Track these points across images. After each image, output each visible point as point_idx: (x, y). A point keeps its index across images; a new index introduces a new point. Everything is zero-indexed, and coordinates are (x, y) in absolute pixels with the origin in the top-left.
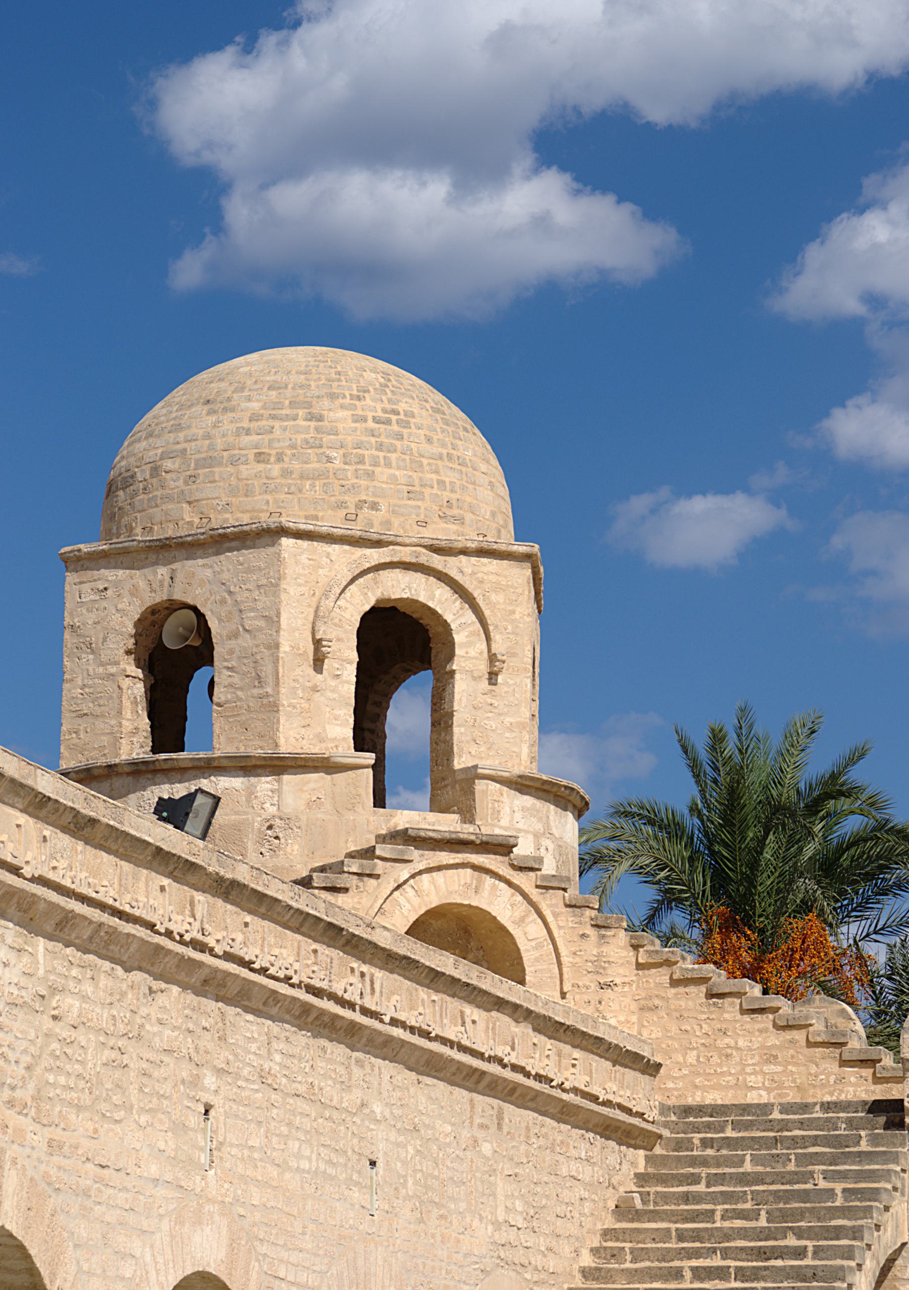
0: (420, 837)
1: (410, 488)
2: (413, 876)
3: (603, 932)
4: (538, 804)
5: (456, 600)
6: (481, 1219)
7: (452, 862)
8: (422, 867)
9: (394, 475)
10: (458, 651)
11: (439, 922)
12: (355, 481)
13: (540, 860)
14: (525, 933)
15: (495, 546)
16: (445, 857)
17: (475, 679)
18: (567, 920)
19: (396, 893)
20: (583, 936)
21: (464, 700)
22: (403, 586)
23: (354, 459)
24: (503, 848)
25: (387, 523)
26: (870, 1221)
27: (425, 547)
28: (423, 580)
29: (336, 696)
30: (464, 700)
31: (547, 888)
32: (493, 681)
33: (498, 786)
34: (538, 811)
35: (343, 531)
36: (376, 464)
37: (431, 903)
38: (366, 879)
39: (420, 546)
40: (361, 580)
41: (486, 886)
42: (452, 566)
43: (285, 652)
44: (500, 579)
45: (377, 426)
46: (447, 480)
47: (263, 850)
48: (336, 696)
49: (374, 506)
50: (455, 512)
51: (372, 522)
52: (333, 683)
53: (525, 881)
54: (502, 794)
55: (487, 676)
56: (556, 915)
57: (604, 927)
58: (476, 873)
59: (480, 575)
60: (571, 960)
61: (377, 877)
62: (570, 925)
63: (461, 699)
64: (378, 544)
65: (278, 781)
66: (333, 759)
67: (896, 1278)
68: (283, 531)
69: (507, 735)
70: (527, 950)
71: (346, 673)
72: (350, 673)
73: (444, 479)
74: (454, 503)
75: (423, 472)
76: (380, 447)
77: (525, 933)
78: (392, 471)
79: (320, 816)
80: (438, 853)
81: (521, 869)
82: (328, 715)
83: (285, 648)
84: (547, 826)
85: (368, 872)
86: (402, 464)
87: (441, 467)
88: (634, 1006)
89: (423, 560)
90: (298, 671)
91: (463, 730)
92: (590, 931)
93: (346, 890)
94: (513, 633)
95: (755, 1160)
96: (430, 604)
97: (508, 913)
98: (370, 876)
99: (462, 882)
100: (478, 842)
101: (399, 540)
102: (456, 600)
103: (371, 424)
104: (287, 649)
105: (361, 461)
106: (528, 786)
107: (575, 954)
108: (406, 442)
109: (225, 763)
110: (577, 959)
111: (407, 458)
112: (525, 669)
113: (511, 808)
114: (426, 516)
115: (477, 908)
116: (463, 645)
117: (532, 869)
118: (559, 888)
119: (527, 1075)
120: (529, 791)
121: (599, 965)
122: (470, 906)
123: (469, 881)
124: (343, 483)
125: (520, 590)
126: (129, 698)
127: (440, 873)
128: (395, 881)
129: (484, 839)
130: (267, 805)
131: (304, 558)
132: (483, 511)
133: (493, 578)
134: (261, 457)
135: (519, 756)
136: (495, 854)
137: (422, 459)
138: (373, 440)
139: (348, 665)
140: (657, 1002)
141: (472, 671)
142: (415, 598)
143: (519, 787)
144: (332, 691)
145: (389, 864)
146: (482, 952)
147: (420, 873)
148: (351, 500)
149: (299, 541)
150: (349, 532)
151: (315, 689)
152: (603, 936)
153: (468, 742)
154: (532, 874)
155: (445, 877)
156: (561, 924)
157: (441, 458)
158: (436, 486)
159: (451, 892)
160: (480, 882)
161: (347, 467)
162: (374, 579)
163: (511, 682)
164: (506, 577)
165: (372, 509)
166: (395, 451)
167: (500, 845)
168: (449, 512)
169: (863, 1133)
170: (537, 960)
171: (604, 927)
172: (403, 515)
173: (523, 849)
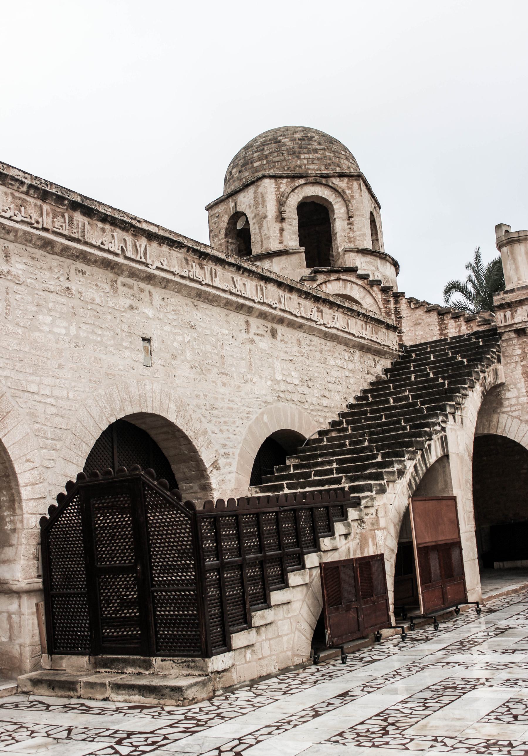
6: (261, 377)
13: (368, 275)
52: (289, 227)
84: (377, 268)
88: (412, 324)
92: (391, 299)
95: (434, 357)
96: (323, 196)
116: (337, 209)
117: (365, 279)
119: (296, 317)
121: (397, 312)
134: (260, 159)
140: (420, 321)
154: (366, 281)
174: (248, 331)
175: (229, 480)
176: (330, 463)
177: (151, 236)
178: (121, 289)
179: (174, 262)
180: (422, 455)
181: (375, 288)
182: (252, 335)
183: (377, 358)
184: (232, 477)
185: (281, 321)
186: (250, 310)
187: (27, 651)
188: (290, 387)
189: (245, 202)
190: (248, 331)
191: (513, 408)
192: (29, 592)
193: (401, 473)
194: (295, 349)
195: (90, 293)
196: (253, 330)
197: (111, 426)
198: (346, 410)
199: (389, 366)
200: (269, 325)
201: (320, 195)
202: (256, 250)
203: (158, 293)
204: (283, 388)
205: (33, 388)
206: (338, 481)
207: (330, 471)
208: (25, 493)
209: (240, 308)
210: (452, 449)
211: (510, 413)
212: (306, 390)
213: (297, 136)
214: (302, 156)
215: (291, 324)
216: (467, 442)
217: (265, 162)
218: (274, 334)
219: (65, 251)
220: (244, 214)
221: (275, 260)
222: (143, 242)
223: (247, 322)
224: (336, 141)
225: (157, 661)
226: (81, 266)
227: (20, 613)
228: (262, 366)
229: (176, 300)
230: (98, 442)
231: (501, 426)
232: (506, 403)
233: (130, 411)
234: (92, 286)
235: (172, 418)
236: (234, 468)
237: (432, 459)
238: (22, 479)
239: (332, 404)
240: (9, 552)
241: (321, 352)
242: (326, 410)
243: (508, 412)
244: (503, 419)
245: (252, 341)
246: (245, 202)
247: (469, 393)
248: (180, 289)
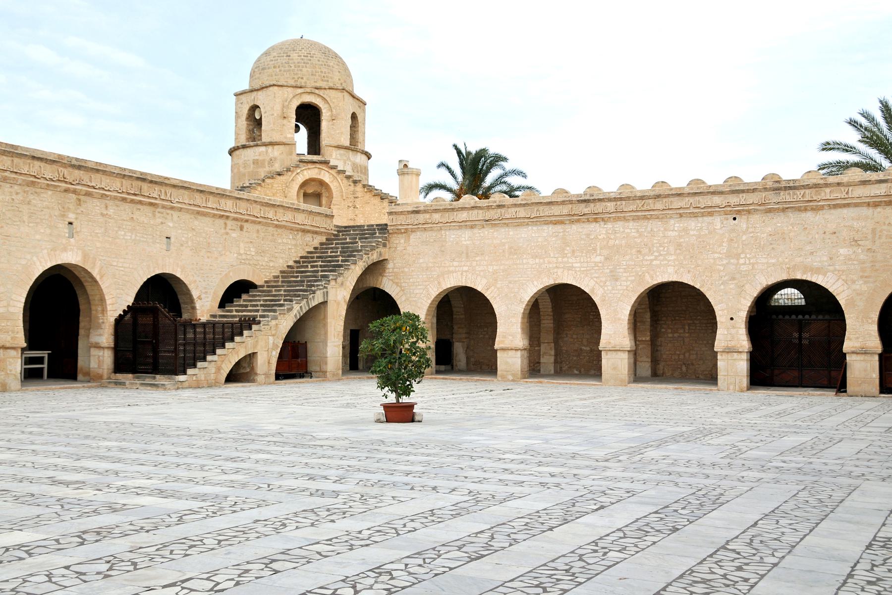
25: (306, 83)
53: (333, 172)
92: (352, 184)
121: (354, 192)
148: (296, 77)
173: (331, 164)
174: (225, 228)
175: (205, 305)
176: (259, 301)
177: (174, 186)
178: (158, 215)
179: (186, 197)
180: (307, 302)
181: (341, 176)
182: (227, 230)
183: (315, 236)
184: (208, 304)
185: (247, 221)
186: (228, 217)
187: (105, 372)
188: (248, 257)
189: (260, 99)
190: (225, 228)
192: (108, 348)
193: (290, 310)
194: (255, 235)
195: (142, 219)
196: (229, 227)
197: (148, 279)
198: (286, 269)
199: (324, 241)
200: (239, 224)
202: (265, 138)
203: (176, 214)
204: (244, 257)
205: (115, 264)
206: (258, 311)
207: (257, 305)
208: (109, 308)
209: (221, 216)
210: (331, 298)
212: (259, 258)
213: (304, 52)
215: (254, 222)
217: (278, 70)
218: (242, 228)
219: (132, 201)
220: (258, 107)
221: (276, 147)
222: (169, 190)
223: (225, 224)
224: (336, 56)
225: (158, 376)
226: (139, 206)
227: (103, 356)
229: (186, 217)
230: (142, 287)
232: (387, 271)
233: (157, 272)
234: (143, 215)
235: (178, 275)
236: (210, 299)
237: (313, 304)
238: (108, 302)
239: (277, 265)
240: (101, 331)
241: (273, 235)
244: (385, 280)
245: (227, 234)
246: (260, 99)
247: (352, 267)
248: (188, 211)
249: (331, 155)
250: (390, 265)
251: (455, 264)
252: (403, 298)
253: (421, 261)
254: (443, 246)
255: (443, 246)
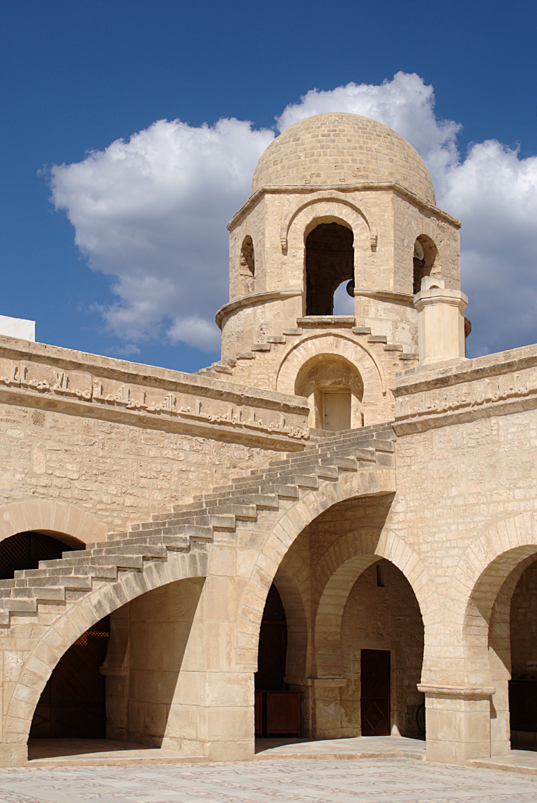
0: (303, 322)
1: (337, 164)
2: (303, 341)
3: (406, 362)
4: (396, 307)
5: (354, 213)
7: (321, 333)
8: (306, 337)
9: (328, 160)
10: (355, 238)
11: (333, 365)
12: (309, 165)
14: (363, 366)
15: (371, 185)
16: (319, 331)
17: (364, 250)
18: (386, 358)
19: (295, 351)
20: (395, 365)
21: (359, 261)
22: (326, 210)
23: (309, 155)
24: (350, 325)
26: (314, 474)
27: (335, 189)
28: (337, 206)
29: (294, 265)
30: (359, 261)
31: (374, 342)
32: (374, 250)
33: (367, 298)
34: (396, 310)
35: (293, 187)
36: (319, 155)
37: (312, 354)
38: (278, 345)
39: (333, 189)
40: (305, 210)
41: (341, 344)
42: (348, 197)
43: (268, 248)
44: (376, 200)
45: (323, 138)
46: (358, 159)
47: (259, 340)
48: (294, 265)
49: (318, 175)
50: (362, 173)
51: (315, 182)
53: (363, 340)
54: (370, 303)
55: (370, 248)
56: (379, 356)
57: (406, 360)
58: (336, 338)
59: (366, 200)
60: (388, 377)
61: (285, 343)
62: (388, 360)
63: (357, 261)
64: (312, 191)
65: (264, 307)
66: (281, 293)
67: (392, 512)
68: (264, 192)
69: (382, 275)
70: (364, 374)
71: (298, 254)
72: (301, 255)
73: (356, 158)
74: (362, 169)
75: (344, 156)
76: (322, 147)
77: (363, 366)
78: (327, 158)
79: (279, 321)
80: (315, 330)
81: (359, 334)
82: (290, 275)
83: (268, 245)
85: (278, 341)
86: (332, 153)
87: (355, 153)
89: (334, 196)
90: (275, 256)
91: (359, 275)
93: (269, 351)
94: (383, 226)
96: (341, 217)
97: (354, 356)
98: (280, 343)
99: (329, 343)
100: (333, 322)
101: (321, 188)
102: (354, 213)
103: (320, 138)
104: (269, 246)
105: (313, 155)
106: (388, 298)
107: (390, 374)
108: (336, 143)
109: (245, 303)
110: (392, 376)
111: (336, 150)
112: (391, 243)
113: (376, 309)
114: (344, 177)
115: (337, 355)
116: (356, 234)
118: (380, 342)
120: (389, 300)
122: (333, 354)
123: (332, 342)
124: (304, 167)
125: (387, 205)
126: (243, 285)
127: (317, 339)
128: (292, 345)
129: (336, 320)
130: (260, 319)
131: (276, 203)
132: (382, 172)
133: (372, 200)
135: (388, 285)
136: (345, 328)
137: (344, 150)
138: (319, 144)
139: (300, 251)
141: (363, 246)
142: (333, 215)
143: (381, 298)
144: (292, 263)
145: (290, 337)
146: (357, 378)
147: (306, 340)
148: (308, 174)
149: (274, 195)
150: (296, 187)
151: (284, 263)
152: (406, 364)
153: (362, 281)
155: (319, 341)
156: (382, 359)
157: (355, 148)
158: (350, 161)
159: (323, 348)
160: (338, 342)
161: (306, 159)
162: (312, 208)
163: (383, 249)
164: (379, 199)
165: (317, 176)
166: (329, 148)
167: (345, 323)
168: (358, 173)
169: (374, 434)
170: (370, 378)
171: (406, 360)
172: (332, 177)
185: (51, 405)
191: (400, 526)
194: (78, 438)
201: (336, 215)
211: (397, 532)
213: (324, 130)
214: (322, 159)
216: (263, 564)
218: (38, 421)
228: (9, 456)
231: (388, 547)
242: (131, 510)
243: (395, 529)
249: (366, 312)
250: (398, 507)
251: (519, 493)
252: (424, 578)
253: (454, 491)
254: (494, 454)
255: (494, 454)
